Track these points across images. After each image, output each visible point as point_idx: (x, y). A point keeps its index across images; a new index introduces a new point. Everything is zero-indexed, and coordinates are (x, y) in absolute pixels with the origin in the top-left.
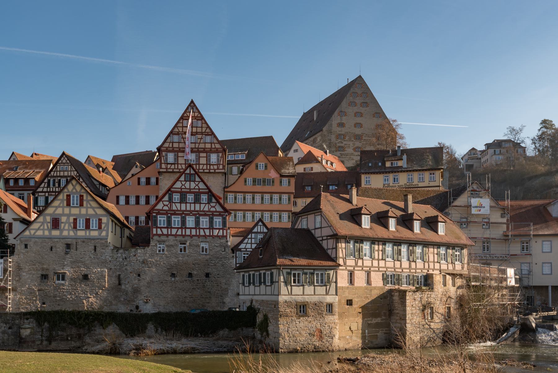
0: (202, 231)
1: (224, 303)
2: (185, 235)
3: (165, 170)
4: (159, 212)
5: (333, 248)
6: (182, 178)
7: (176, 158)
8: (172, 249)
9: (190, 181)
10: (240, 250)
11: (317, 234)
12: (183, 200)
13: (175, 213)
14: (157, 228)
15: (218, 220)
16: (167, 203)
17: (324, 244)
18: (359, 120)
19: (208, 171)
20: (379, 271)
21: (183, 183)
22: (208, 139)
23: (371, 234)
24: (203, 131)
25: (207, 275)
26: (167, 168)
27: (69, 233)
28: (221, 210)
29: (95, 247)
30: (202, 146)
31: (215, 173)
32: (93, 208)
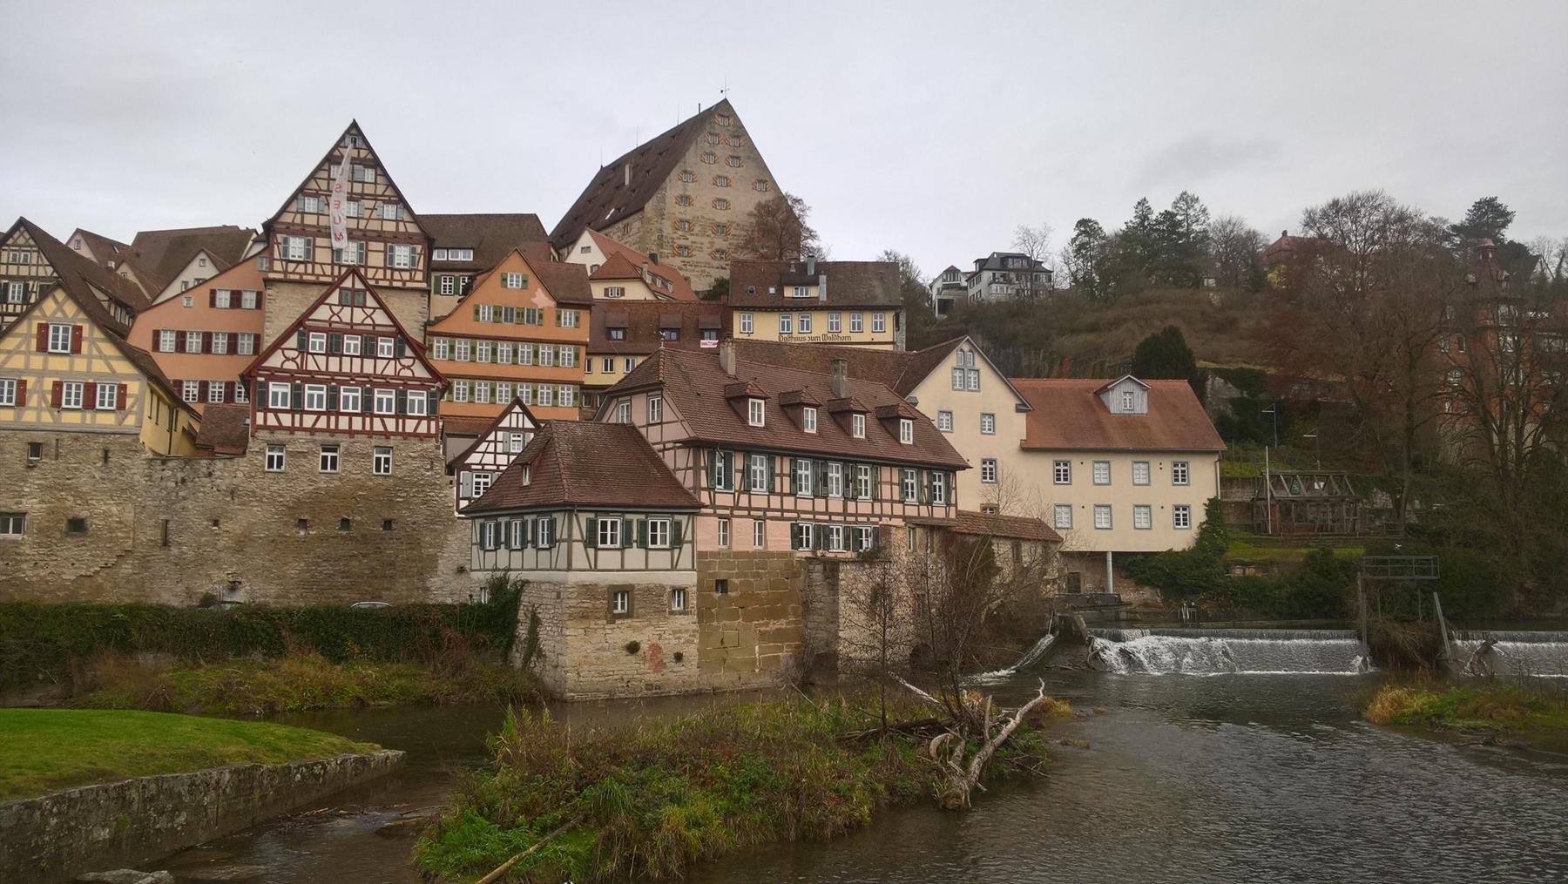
0: (377, 421)
1: (427, 590)
2: (337, 431)
3: (281, 276)
4: (276, 375)
5: (688, 468)
6: (334, 298)
7: (310, 250)
8: (304, 461)
9: (353, 306)
10: (468, 468)
11: (653, 435)
12: (334, 349)
14: (267, 410)
15: (418, 398)
16: (294, 354)
17: (668, 459)
18: (722, 193)
19: (386, 284)
20: (782, 519)
21: (336, 309)
22: (390, 211)
23: (767, 440)
24: (379, 192)
26: (285, 272)
27: (39, 417)
28: (426, 375)
29: (106, 452)
30: (374, 226)
31: (403, 289)
32: (105, 358)
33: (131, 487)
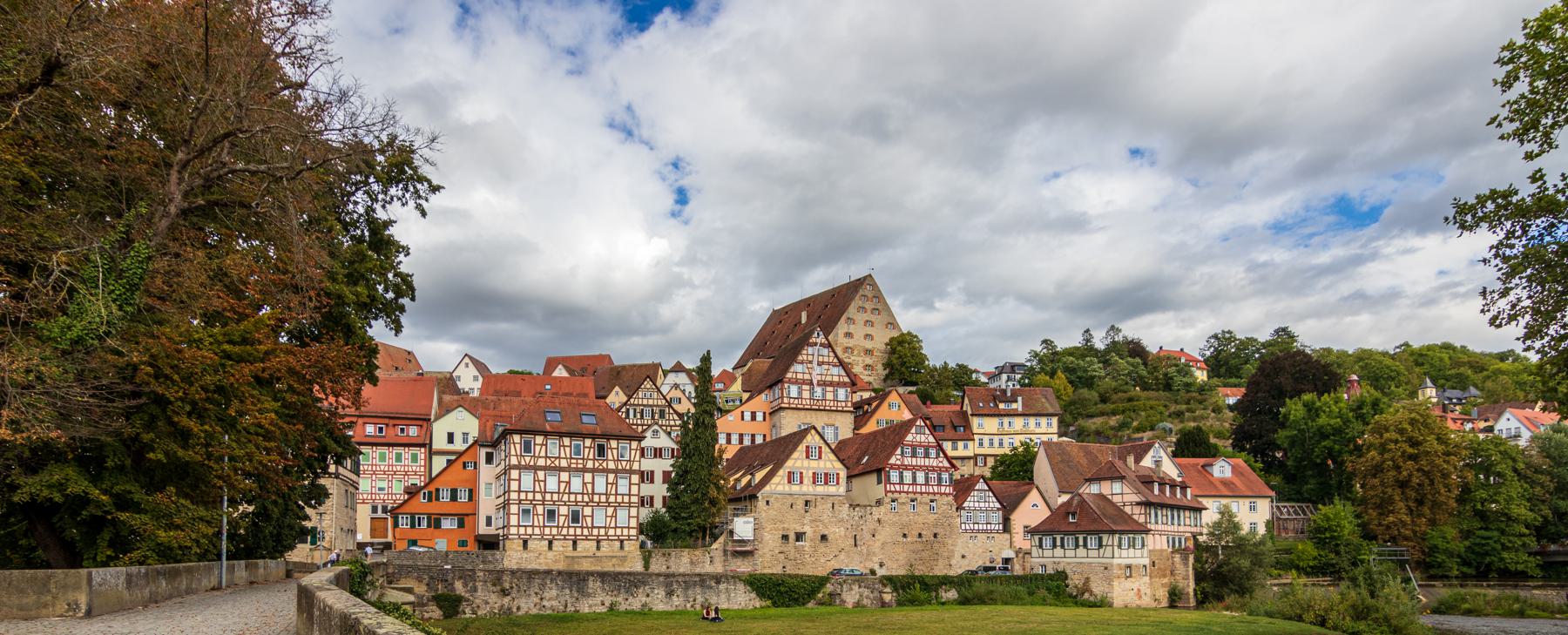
13: (906, 468)
18: (869, 330)
25: (935, 535)
30: (829, 378)
33: (842, 520)
